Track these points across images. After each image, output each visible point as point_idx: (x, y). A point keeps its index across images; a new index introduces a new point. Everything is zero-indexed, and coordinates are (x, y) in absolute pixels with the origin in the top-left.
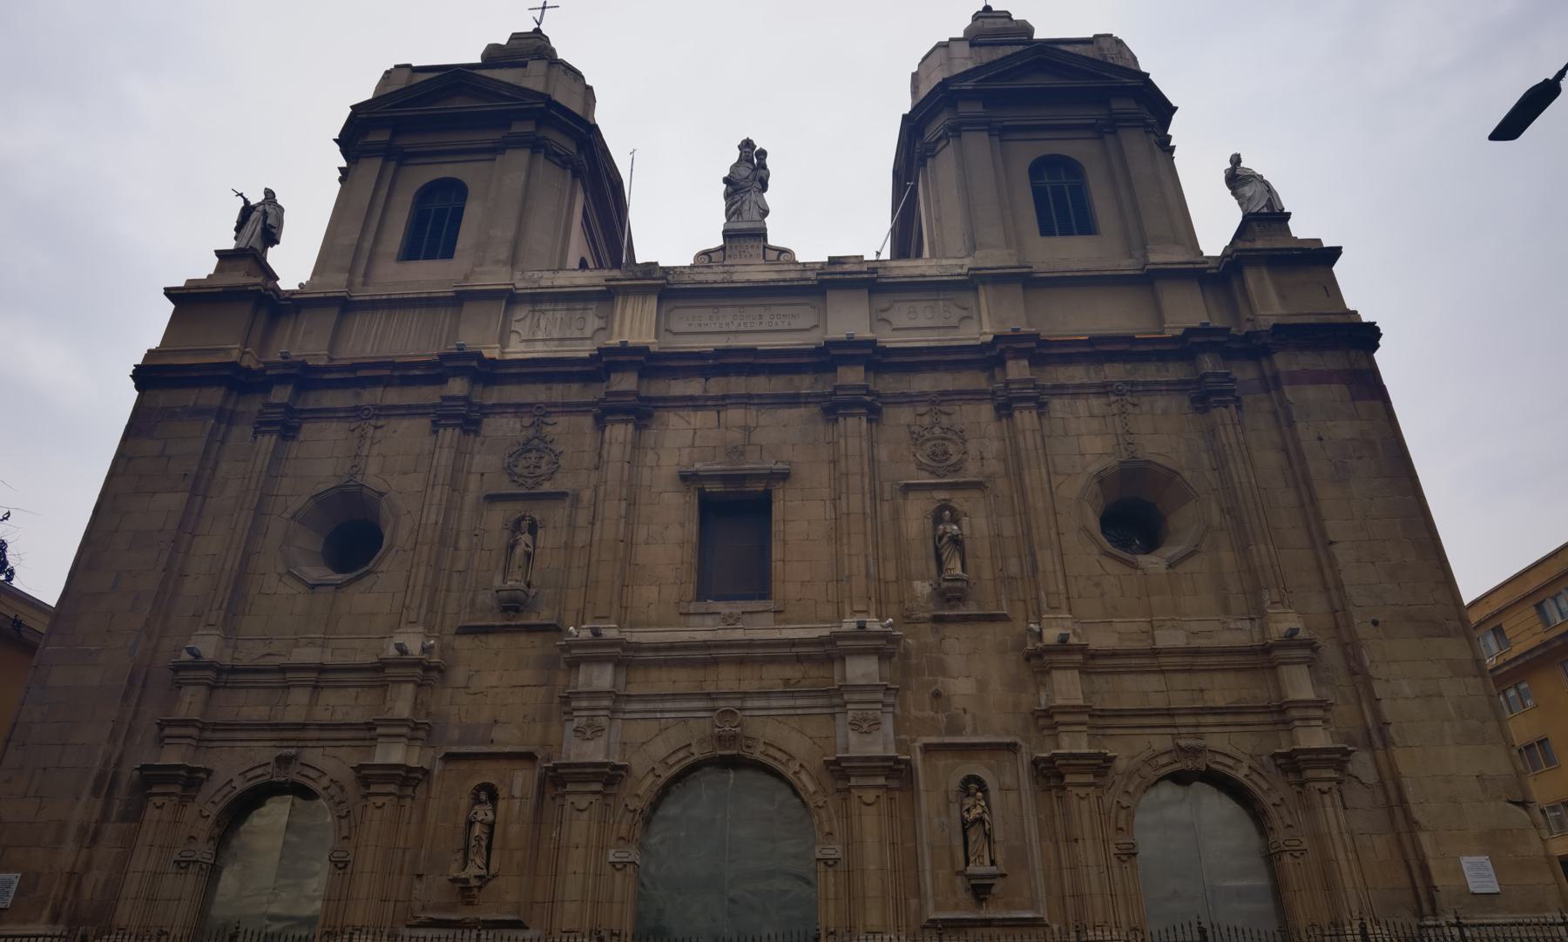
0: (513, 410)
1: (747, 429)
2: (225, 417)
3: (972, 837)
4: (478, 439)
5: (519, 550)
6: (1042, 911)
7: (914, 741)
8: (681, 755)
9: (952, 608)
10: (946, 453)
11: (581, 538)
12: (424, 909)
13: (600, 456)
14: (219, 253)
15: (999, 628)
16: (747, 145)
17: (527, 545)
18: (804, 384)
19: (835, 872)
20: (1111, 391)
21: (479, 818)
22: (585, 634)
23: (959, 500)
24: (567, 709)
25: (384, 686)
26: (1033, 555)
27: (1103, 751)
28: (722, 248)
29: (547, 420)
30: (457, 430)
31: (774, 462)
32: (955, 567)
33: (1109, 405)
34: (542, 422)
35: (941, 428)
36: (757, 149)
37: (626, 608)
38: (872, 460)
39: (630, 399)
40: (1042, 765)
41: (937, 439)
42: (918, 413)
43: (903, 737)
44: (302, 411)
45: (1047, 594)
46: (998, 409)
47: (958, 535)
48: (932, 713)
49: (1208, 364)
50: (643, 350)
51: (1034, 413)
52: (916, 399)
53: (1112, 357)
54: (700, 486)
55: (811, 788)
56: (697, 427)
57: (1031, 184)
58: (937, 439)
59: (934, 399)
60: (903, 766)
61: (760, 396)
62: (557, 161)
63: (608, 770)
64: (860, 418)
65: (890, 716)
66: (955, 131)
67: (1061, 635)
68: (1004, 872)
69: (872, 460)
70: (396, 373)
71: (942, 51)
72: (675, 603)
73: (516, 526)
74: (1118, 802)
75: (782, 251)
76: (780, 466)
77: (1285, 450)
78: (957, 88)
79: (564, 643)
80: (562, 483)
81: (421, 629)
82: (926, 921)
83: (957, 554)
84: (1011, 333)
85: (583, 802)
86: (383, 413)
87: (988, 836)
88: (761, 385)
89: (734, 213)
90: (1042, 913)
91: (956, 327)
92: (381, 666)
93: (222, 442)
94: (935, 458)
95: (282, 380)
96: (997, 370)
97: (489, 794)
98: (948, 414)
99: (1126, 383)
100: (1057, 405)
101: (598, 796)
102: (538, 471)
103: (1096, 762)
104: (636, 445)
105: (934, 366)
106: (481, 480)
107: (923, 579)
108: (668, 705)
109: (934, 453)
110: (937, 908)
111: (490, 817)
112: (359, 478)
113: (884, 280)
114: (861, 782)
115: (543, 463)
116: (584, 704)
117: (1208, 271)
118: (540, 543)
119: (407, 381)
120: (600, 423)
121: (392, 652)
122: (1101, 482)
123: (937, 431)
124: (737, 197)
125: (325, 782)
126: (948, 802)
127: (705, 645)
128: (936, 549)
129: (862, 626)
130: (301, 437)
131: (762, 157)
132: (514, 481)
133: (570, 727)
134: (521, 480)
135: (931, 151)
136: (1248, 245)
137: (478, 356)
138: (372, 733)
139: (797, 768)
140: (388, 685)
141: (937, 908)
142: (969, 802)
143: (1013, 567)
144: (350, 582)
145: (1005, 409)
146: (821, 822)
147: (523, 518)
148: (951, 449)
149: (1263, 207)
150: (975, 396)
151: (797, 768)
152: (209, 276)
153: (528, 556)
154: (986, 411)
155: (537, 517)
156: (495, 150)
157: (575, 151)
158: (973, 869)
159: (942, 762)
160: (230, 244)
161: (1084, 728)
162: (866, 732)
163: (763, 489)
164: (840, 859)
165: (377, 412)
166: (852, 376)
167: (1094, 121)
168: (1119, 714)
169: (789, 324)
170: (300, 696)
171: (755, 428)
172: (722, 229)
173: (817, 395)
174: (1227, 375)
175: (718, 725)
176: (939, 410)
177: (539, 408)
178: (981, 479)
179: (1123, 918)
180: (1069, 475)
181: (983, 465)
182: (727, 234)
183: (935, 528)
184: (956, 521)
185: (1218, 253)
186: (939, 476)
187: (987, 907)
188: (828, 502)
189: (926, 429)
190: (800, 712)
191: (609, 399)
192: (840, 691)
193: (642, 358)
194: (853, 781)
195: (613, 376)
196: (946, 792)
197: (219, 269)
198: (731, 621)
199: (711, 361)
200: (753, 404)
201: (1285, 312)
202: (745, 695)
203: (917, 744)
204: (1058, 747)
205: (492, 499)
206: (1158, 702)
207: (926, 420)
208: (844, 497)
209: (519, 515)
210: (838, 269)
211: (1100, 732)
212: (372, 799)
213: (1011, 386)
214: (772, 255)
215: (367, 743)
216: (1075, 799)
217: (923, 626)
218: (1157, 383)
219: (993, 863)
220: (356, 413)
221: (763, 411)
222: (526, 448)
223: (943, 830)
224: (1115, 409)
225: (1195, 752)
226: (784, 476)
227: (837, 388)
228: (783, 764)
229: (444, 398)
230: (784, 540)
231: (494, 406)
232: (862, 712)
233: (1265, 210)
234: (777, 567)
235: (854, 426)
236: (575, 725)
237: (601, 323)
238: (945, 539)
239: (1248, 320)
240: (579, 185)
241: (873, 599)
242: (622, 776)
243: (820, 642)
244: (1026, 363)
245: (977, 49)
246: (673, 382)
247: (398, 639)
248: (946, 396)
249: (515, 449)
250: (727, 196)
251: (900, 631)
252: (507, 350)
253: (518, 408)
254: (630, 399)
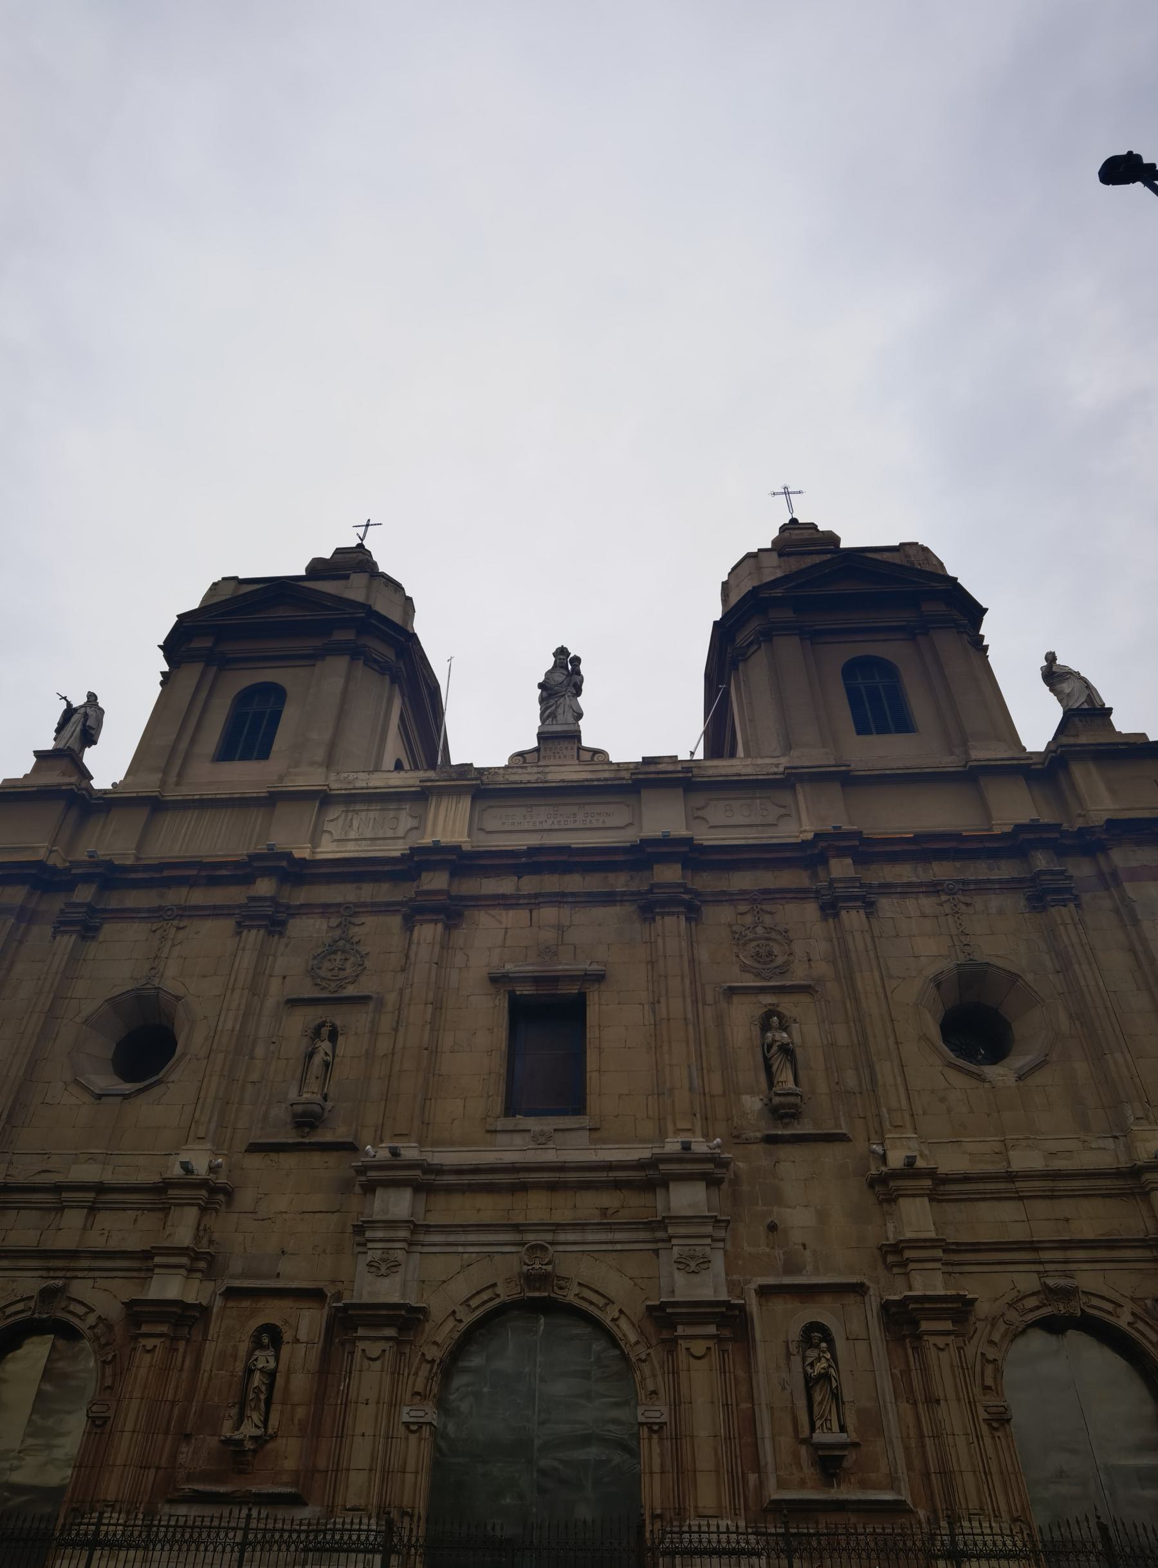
0: (321, 910)
1: (560, 928)
2: (26, 916)
3: (817, 1397)
4: (282, 940)
5: (317, 1059)
6: (903, 1491)
7: (748, 1282)
8: (485, 1296)
9: (786, 1126)
10: (770, 954)
11: (383, 1045)
12: (190, 1478)
13: (407, 957)
14: (39, 755)
15: (838, 1148)
16: (562, 652)
17: (326, 1054)
18: (620, 882)
19: (661, 1439)
20: (942, 890)
21: (260, 1366)
22: (383, 1154)
23: (788, 1005)
24: (358, 1239)
25: (166, 1210)
26: (871, 1067)
27: (961, 1293)
28: (537, 750)
29: (353, 920)
30: (262, 931)
31: (588, 962)
32: (786, 1079)
34: (350, 923)
35: (765, 928)
36: (571, 656)
37: (428, 1124)
38: (692, 960)
39: (441, 898)
40: (893, 1310)
41: (760, 939)
42: (739, 911)
43: (735, 1277)
44: (105, 911)
46: (823, 908)
47: (788, 1044)
48: (768, 1250)
49: (1042, 861)
50: (455, 849)
51: (862, 912)
52: (736, 897)
53: (941, 855)
54: (510, 989)
55: (633, 1337)
56: (509, 926)
57: (845, 684)
58: (760, 939)
59: (756, 897)
60: (737, 1312)
61: (573, 894)
62: (376, 667)
63: (403, 1312)
64: (678, 917)
65: (721, 1252)
66: (767, 636)
67: (908, 1157)
68: (857, 1440)
69: (692, 960)
70: (203, 873)
71: (751, 561)
72: (482, 1119)
73: (317, 1033)
74: (983, 1354)
75: (596, 752)
76: (595, 967)
77: (1132, 950)
78: (767, 595)
79: (360, 1164)
80: (366, 986)
81: (209, 1146)
82: (767, 1501)
83: (788, 1065)
84: (833, 831)
85: (374, 1349)
86: (187, 913)
87: (836, 1396)
88: (575, 883)
89: (548, 717)
90: (905, 1496)
91: (775, 825)
92: (163, 1187)
93: (21, 942)
94: (759, 959)
95: (87, 879)
96: (819, 868)
97: (271, 1337)
98: (770, 913)
99: (957, 881)
100: (886, 905)
101: (391, 1344)
102: (342, 974)
103: (955, 1305)
104: (445, 946)
105: (753, 864)
106: (283, 983)
107: (752, 1093)
108: (472, 1238)
109: (758, 954)
110: (782, 1484)
111: (272, 1365)
112: (156, 982)
113: (699, 779)
114: (690, 1331)
115: (348, 965)
116: (380, 1234)
117: (1033, 767)
118: (340, 1050)
119: (214, 881)
120: (409, 924)
121: (177, 1171)
122: (938, 986)
123: (760, 930)
124: (552, 702)
125: (91, 1319)
126: (789, 1354)
127: (513, 1168)
128: (765, 1057)
129: (686, 1147)
130: (101, 938)
131: (576, 663)
132: (317, 985)
133: (363, 1260)
134: (324, 984)
135: (742, 656)
136: (1072, 741)
137: (288, 856)
138: (150, 1264)
139: (617, 1315)
140: (170, 1208)
141: (782, 1484)
142: (812, 1354)
143: (850, 1079)
144: (140, 1091)
145: (830, 908)
146: (643, 1379)
147: (323, 1025)
148: (776, 949)
149: (1083, 703)
150: (800, 895)
151: (617, 1315)
152: (26, 776)
153: (327, 1065)
154: (811, 910)
155: (338, 1023)
156: (314, 657)
157: (393, 658)
158: (819, 1437)
159: (779, 1306)
160: (48, 744)
161: (938, 1265)
162: (693, 1272)
163: (576, 991)
164: (666, 1423)
165: (180, 913)
166: (669, 874)
167: (905, 623)
168: (976, 1248)
169: (604, 822)
170: (74, 1219)
171: (569, 927)
172: (537, 732)
173: (632, 894)
174: (1062, 872)
175: (527, 1261)
176: (761, 909)
177: (347, 908)
178: (811, 983)
179: (1003, 1507)
180: (904, 979)
181: (810, 967)
182: (541, 736)
183: (763, 1036)
184: (785, 1028)
185: (1041, 748)
186: (765, 979)
187: (839, 1486)
188: (646, 1007)
189: (749, 928)
190: (619, 1247)
191: (418, 899)
192: (663, 1224)
193: (454, 857)
194: (680, 1330)
195: (424, 875)
196: (787, 1343)
197: (35, 769)
198: (542, 1140)
199: (524, 859)
200: (566, 902)
201: (1117, 807)
202: (558, 1227)
203: (753, 1286)
204: (910, 1289)
205: (294, 1003)
206: (1018, 1233)
207: (748, 919)
208: (663, 1000)
209: (320, 1021)
210: (652, 768)
211: (957, 1269)
212: (143, 1342)
213: (836, 885)
214: (586, 756)
215: (142, 1275)
216: (933, 1349)
217: (754, 1147)
218: (989, 881)
219: (843, 1429)
220: (158, 914)
221: (577, 909)
222: (332, 949)
223: (784, 1388)
224: (947, 908)
225: (1067, 1294)
226: (599, 978)
227: (653, 886)
228: (600, 1308)
229: (252, 899)
230: (599, 1048)
231: (302, 905)
232: (688, 1248)
233: (1086, 706)
235: (672, 925)
236: (369, 1259)
237: (415, 823)
238: (775, 1048)
239: (1080, 815)
240: (397, 687)
241: (698, 1116)
242: (419, 1320)
243: (640, 1165)
244: (849, 861)
245: (785, 558)
246: (485, 881)
247: (184, 1157)
248: (768, 895)
249: (319, 951)
250: (542, 700)
251: (729, 1153)
252: (318, 850)
253: (326, 909)
254: (441, 898)
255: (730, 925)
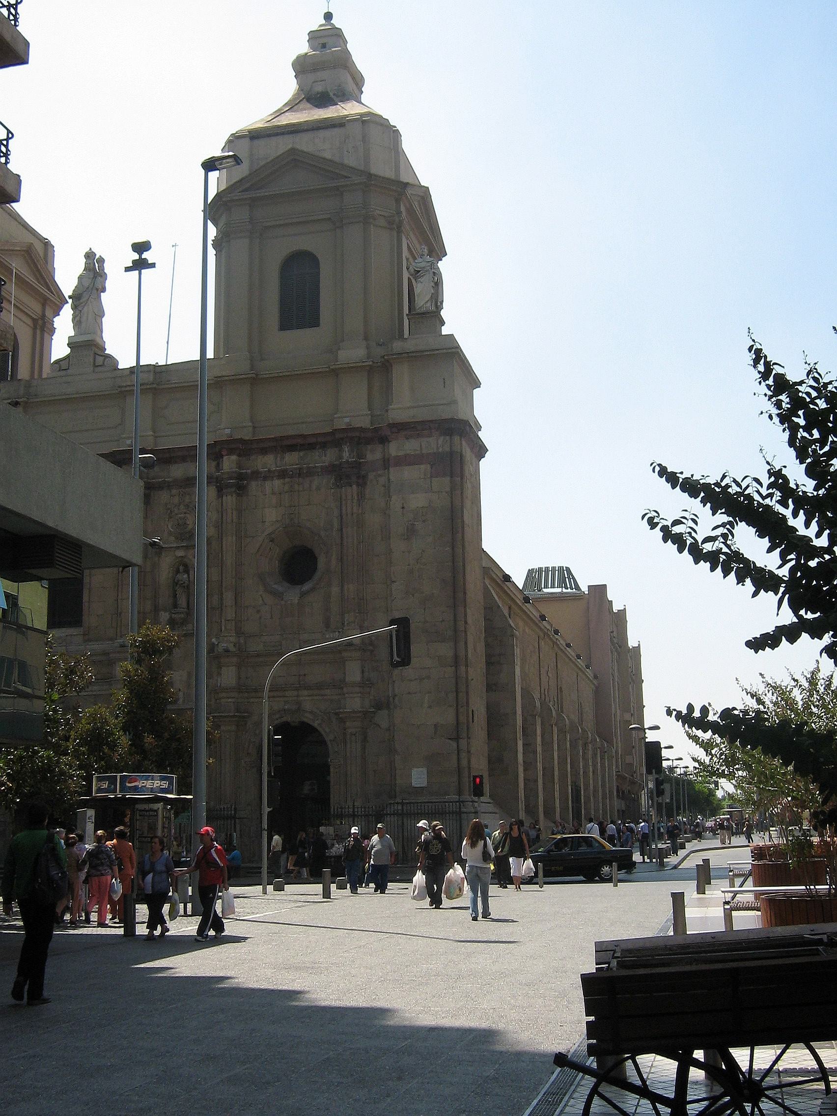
26: (222, 594)
32: (182, 601)
33: (284, 484)
45: (226, 620)
53: (292, 448)
107: (165, 610)
123: (182, 507)
224: (286, 488)
234: (85, 606)
255: (166, 504)
